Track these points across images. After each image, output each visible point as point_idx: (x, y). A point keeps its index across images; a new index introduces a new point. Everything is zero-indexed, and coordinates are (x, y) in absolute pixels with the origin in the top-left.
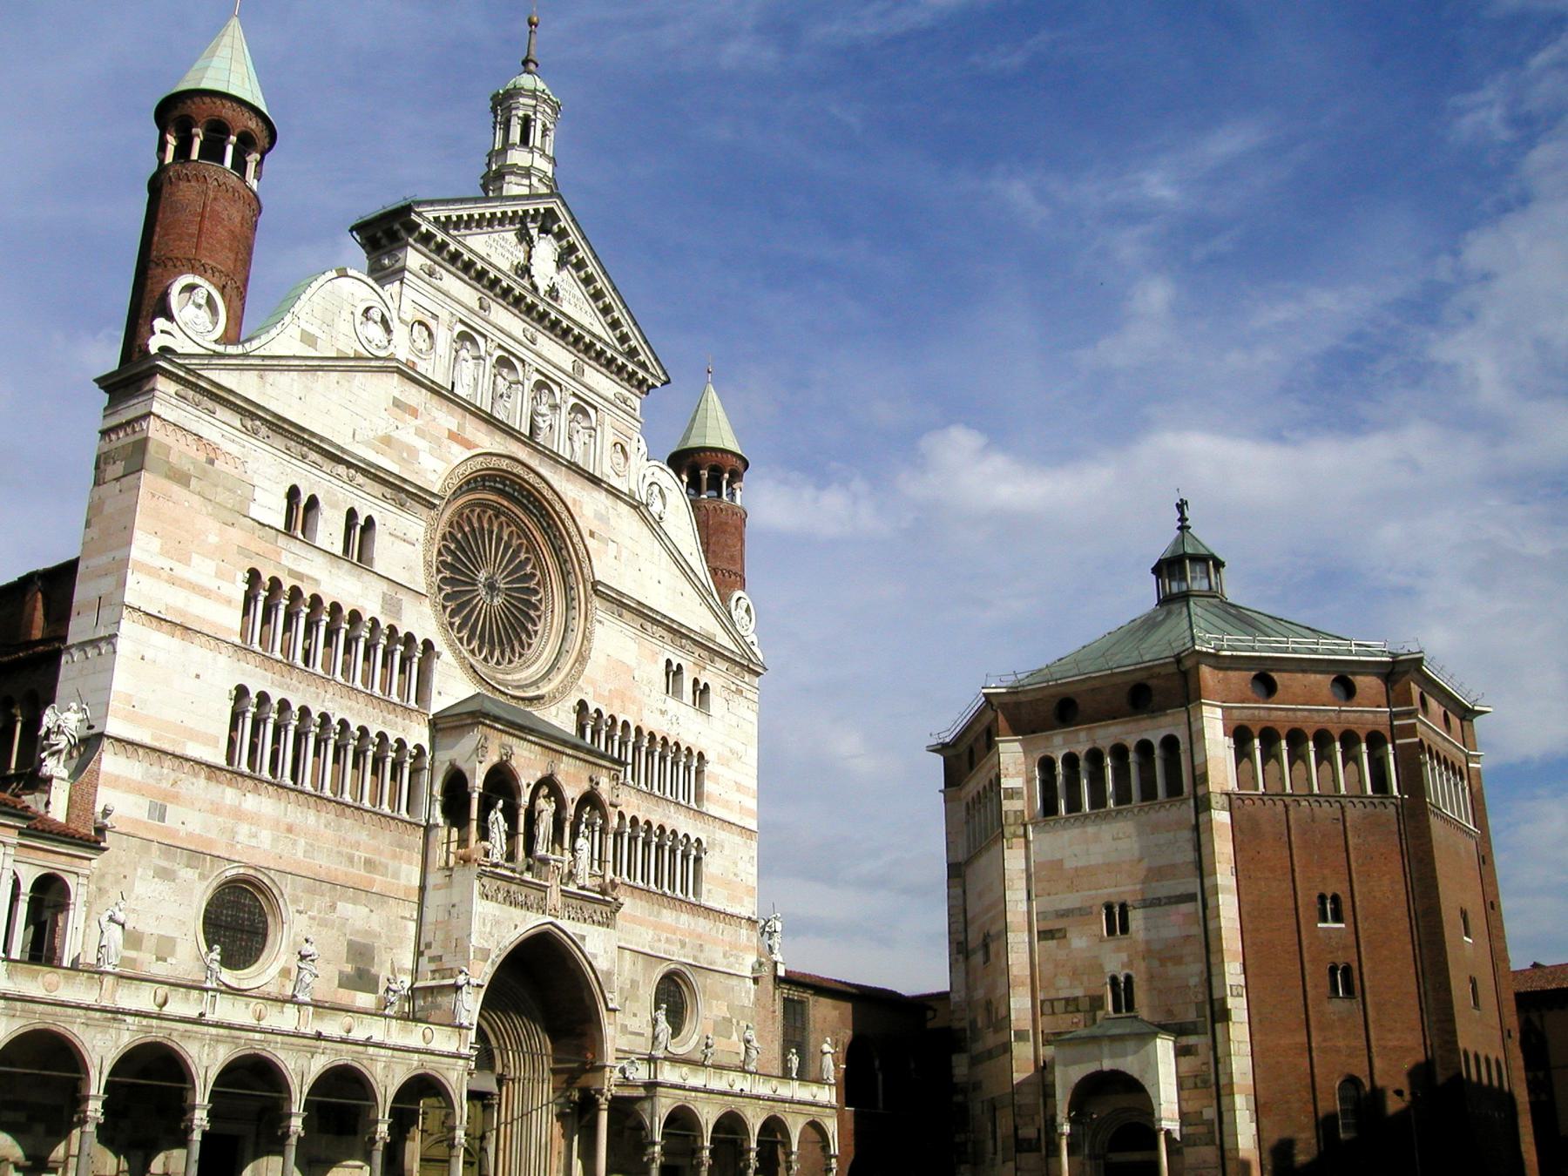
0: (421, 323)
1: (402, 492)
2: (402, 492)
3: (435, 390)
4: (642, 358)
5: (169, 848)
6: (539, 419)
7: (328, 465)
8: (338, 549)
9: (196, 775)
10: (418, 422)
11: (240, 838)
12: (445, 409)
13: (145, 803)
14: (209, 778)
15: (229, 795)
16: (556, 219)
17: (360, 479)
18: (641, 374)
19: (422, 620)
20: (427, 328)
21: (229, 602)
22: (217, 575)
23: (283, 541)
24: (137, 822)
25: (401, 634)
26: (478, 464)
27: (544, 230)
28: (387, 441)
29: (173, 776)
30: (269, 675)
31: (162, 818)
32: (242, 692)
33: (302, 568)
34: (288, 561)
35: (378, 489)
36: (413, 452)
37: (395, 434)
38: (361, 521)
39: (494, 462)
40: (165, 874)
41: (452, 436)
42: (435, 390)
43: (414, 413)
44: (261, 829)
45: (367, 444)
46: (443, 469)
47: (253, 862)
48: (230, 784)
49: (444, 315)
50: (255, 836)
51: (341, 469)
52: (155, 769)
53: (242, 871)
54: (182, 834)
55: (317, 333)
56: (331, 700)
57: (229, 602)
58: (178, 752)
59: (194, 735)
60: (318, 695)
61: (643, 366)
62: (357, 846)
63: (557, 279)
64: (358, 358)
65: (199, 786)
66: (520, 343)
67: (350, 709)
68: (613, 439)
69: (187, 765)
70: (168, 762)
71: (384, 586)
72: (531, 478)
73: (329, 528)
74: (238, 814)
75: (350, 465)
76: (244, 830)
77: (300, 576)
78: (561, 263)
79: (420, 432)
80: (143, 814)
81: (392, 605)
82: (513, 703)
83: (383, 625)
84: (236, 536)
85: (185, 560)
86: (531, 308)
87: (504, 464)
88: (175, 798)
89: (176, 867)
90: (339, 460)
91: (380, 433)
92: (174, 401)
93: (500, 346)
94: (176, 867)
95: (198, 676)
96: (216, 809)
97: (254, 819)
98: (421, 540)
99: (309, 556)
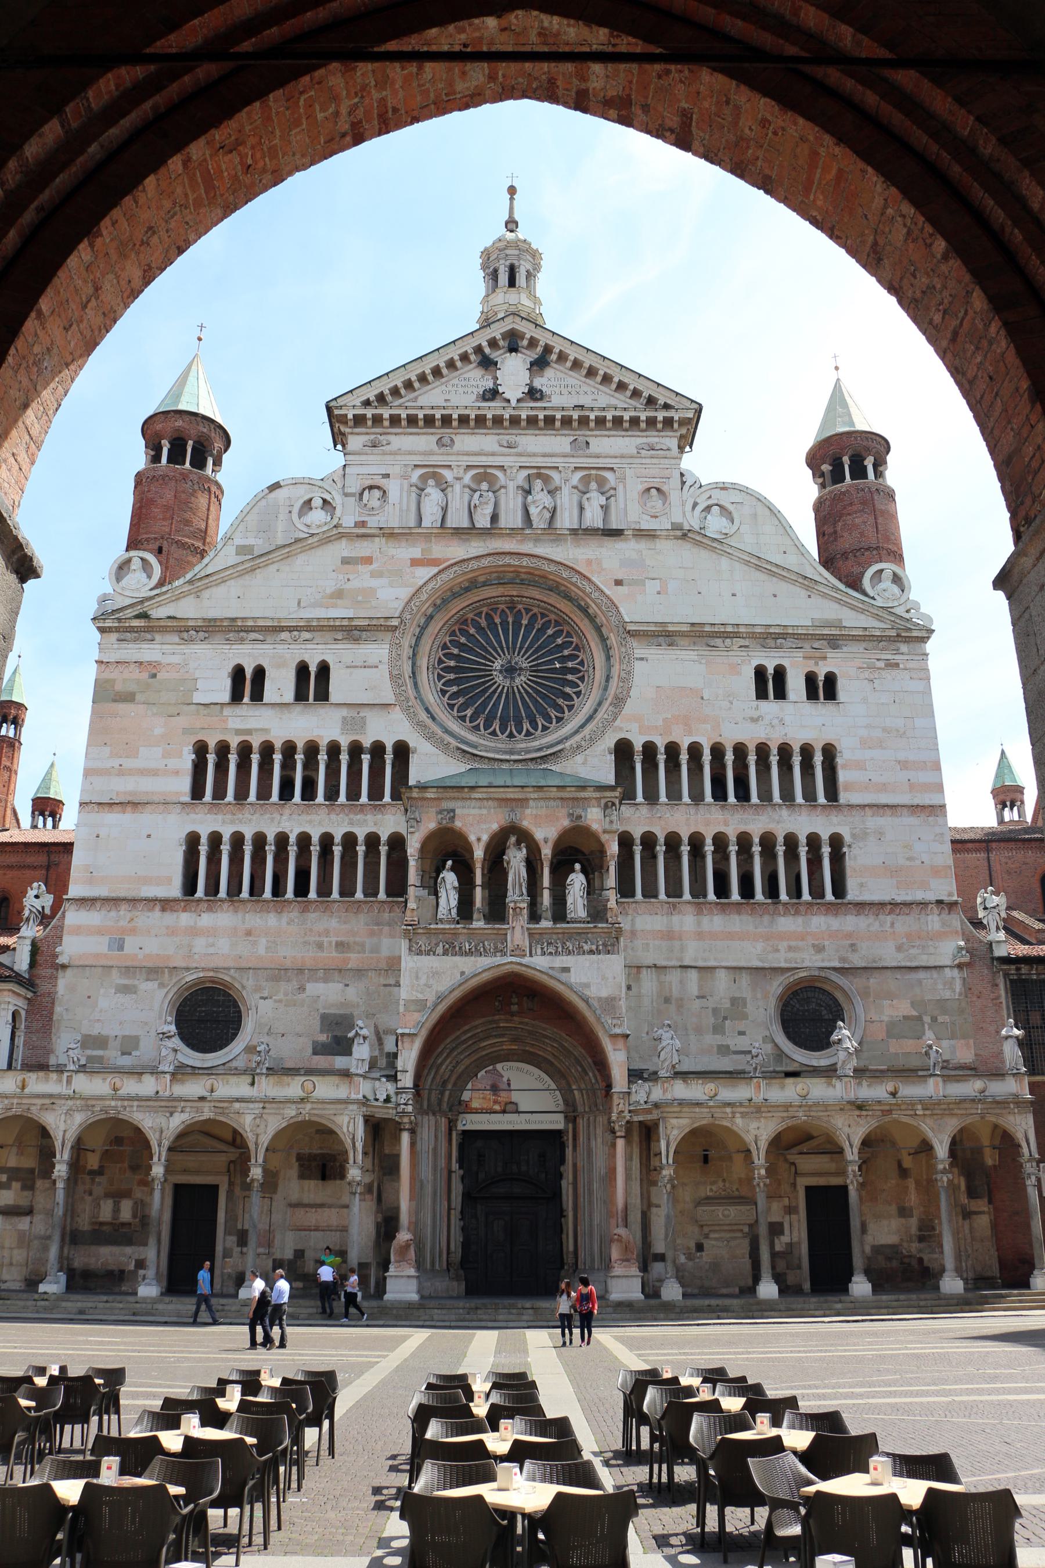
0: (371, 488)
1: (352, 632)
2: (352, 632)
3: (389, 534)
4: (661, 402)
5: (128, 970)
6: (533, 511)
7: (269, 639)
8: (289, 696)
9: (152, 910)
10: (374, 566)
11: (195, 950)
12: (404, 544)
13: (105, 940)
14: (163, 910)
15: (185, 919)
16: (522, 336)
17: (306, 635)
18: (660, 415)
19: (387, 729)
20: (378, 488)
21: (177, 773)
22: (164, 757)
23: (228, 711)
24: (97, 956)
25: (367, 743)
26: (449, 575)
27: (513, 349)
28: (339, 594)
29: (129, 915)
30: (220, 817)
31: (121, 948)
32: (193, 840)
33: (251, 724)
34: (234, 723)
35: (329, 636)
36: (371, 592)
37: (348, 586)
38: (313, 669)
39: (473, 565)
40: (126, 990)
41: (415, 563)
42: (389, 534)
43: (368, 560)
44: (223, 939)
45: (314, 605)
46: (405, 593)
47: (212, 965)
48: (184, 910)
49: (395, 470)
50: (213, 945)
51: (284, 635)
52: (113, 914)
53: (201, 975)
54: (140, 957)
55: (250, 541)
56: (289, 820)
57: (177, 773)
58: (130, 894)
59: (147, 881)
60: (272, 820)
61: (667, 406)
62: (327, 933)
63: (538, 383)
64: (298, 541)
65: (155, 918)
66: (493, 454)
67: (310, 822)
68: (641, 487)
69: (140, 906)
70: (124, 906)
71: (344, 712)
72: (525, 562)
73: (280, 685)
74: (194, 932)
75: (290, 629)
76: (200, 945)
77: (249, 732)
78: (540, 364)
79: (376, 575)
80: (104, 949)
81: (347, 724)
82: (531, 765)
83: (344, 743)
84: (181, 722)
85: (135, 755)
86: (498, 421)
87: (485, 562)
88: (133, 931)
89: (136, 982)
90: (282, 629)
91: (328, 591)
92: (115, 646)
93: (469, 467)
94: (136, 982)
95: (149, 836)
96: (172, 932)
97: (212, 932)
98: (386, 659)
99: (257, 713)
